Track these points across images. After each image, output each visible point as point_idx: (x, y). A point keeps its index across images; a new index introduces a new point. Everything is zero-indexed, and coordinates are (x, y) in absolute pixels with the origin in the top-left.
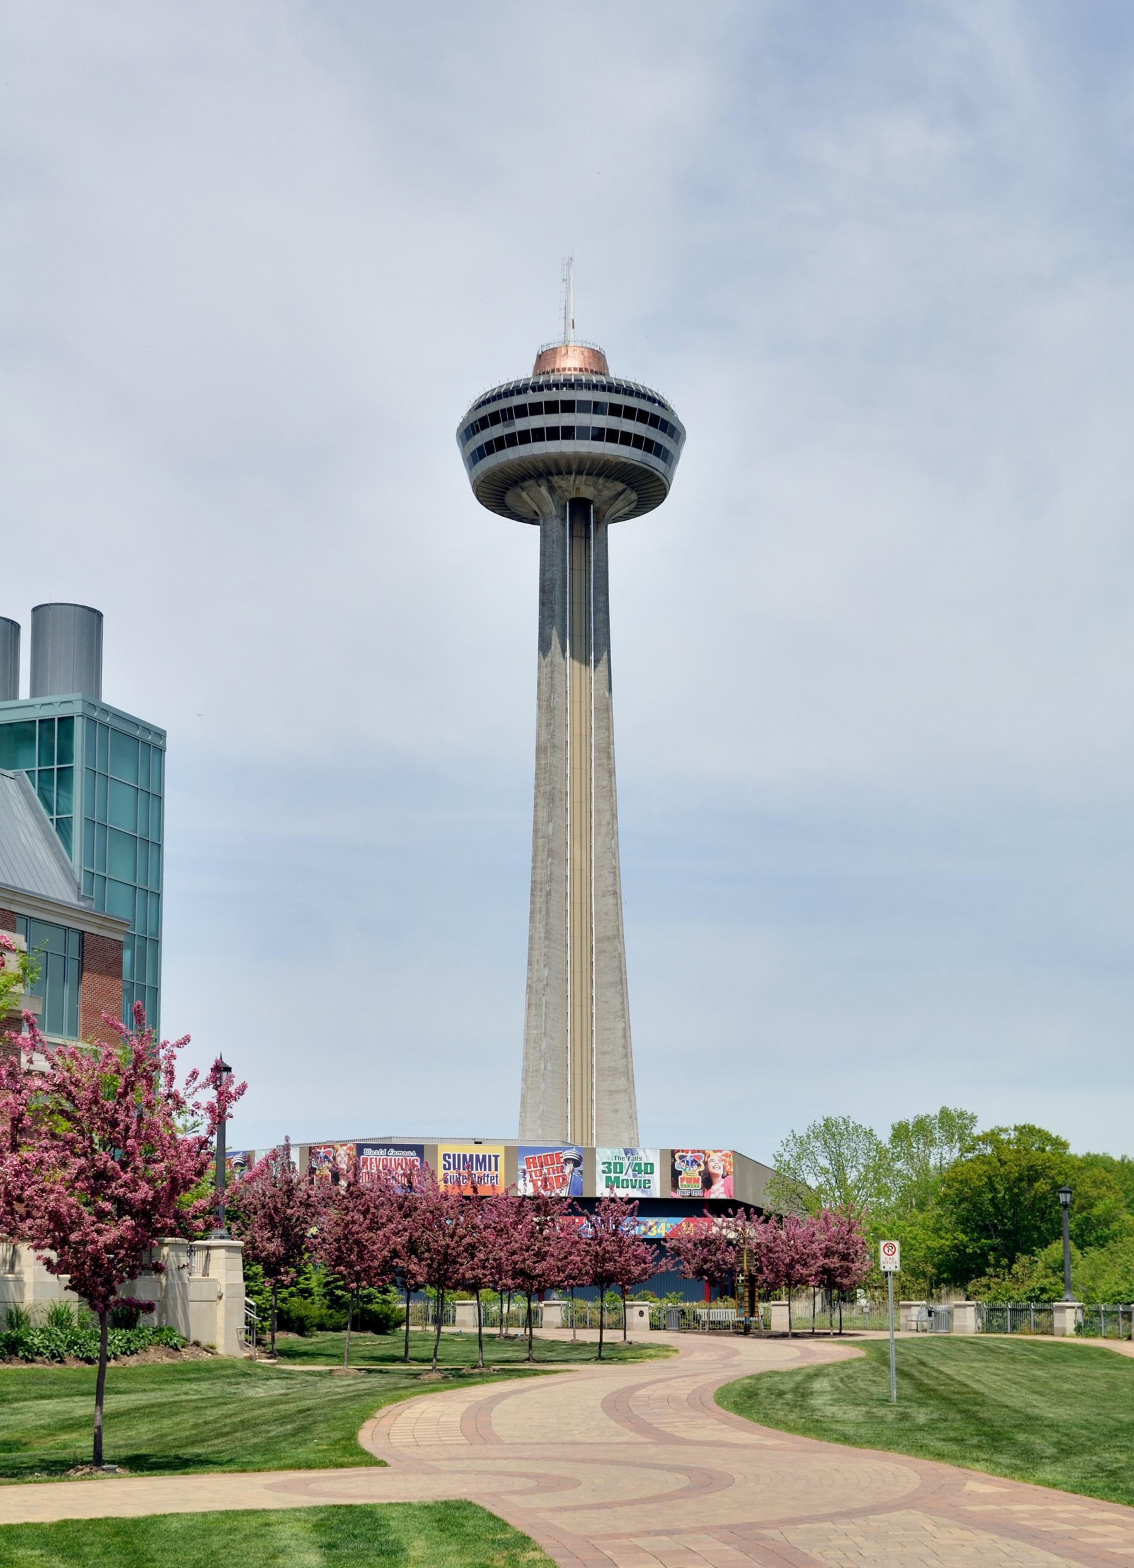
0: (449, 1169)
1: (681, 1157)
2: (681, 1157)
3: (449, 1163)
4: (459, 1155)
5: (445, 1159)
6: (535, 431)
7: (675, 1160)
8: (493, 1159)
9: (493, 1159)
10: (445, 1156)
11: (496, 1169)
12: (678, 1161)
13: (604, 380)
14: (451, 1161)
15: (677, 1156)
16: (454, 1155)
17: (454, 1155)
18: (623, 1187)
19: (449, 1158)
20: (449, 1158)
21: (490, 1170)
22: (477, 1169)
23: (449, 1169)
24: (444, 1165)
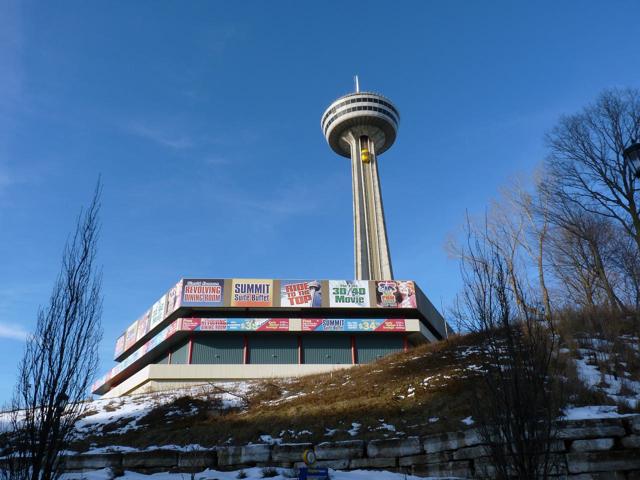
0: (239, 292)
1: (381, 285)
2: (381, 285)
3: (239, 289)
4: (245, 285)
7: (378, 287)
8: (266, 287)
9: (266, 287)
10: (236, 285)
12: (380, 287)
14: (240, 288)
15: (379, 284)
16: (242, 285)
17: (242, 285)
19: (239, 286)
21: (264, 292)
22: (256, 292)
23: (239, 292)
24: (236, 290)
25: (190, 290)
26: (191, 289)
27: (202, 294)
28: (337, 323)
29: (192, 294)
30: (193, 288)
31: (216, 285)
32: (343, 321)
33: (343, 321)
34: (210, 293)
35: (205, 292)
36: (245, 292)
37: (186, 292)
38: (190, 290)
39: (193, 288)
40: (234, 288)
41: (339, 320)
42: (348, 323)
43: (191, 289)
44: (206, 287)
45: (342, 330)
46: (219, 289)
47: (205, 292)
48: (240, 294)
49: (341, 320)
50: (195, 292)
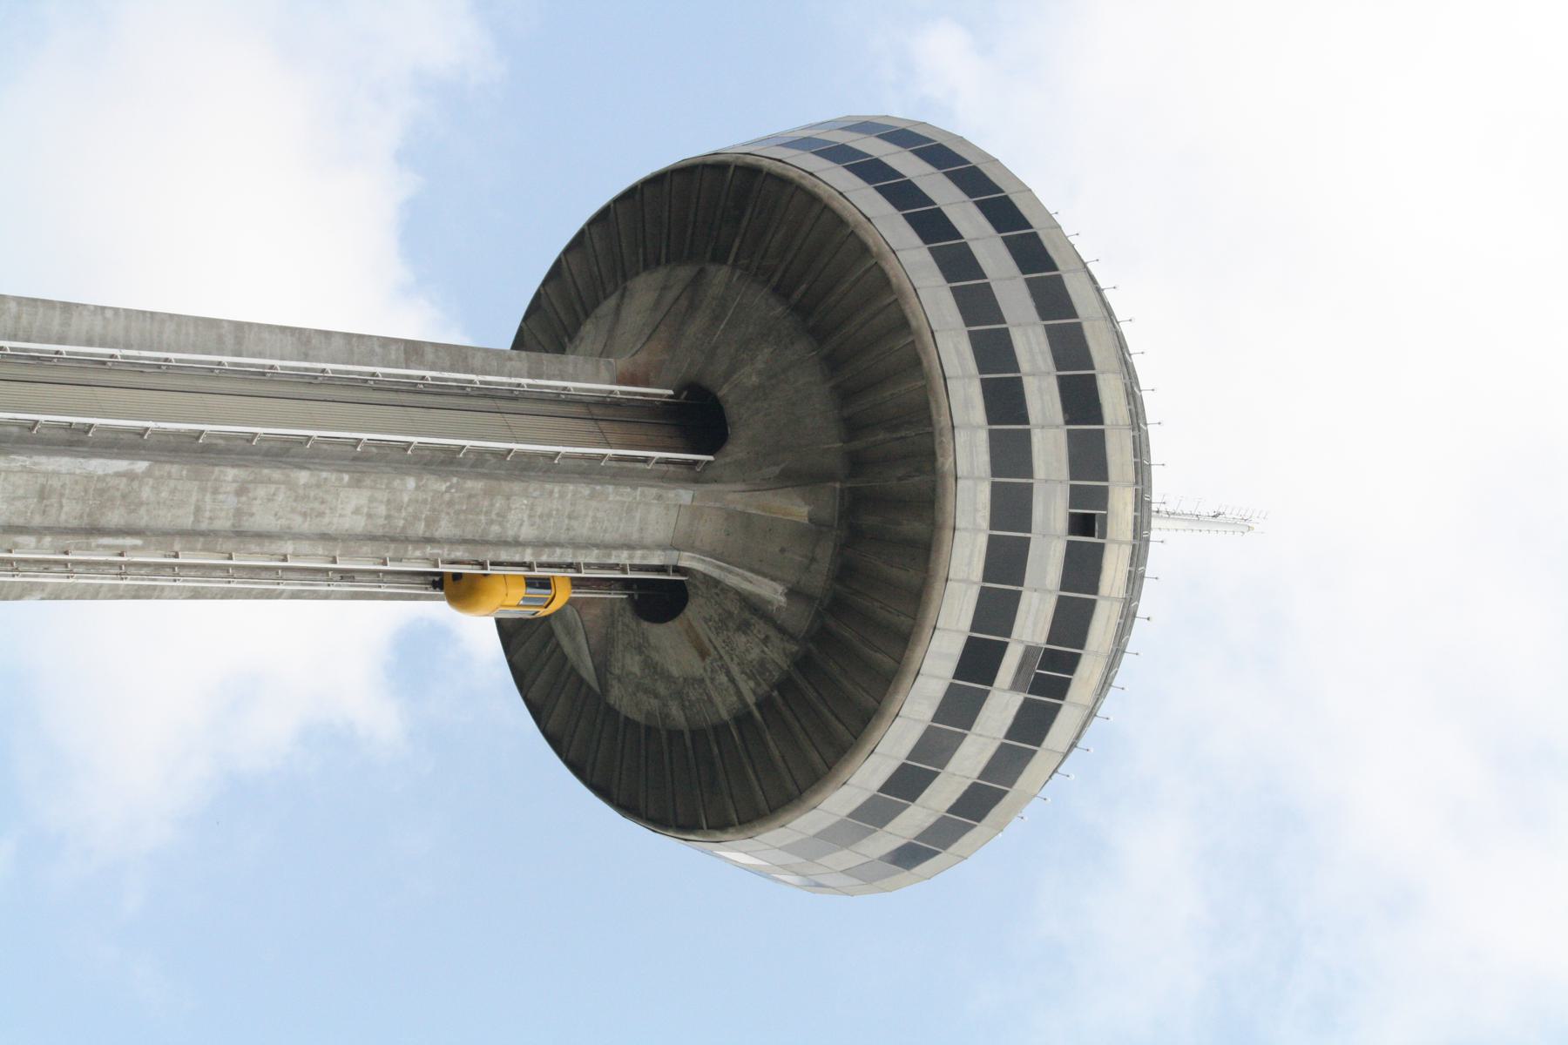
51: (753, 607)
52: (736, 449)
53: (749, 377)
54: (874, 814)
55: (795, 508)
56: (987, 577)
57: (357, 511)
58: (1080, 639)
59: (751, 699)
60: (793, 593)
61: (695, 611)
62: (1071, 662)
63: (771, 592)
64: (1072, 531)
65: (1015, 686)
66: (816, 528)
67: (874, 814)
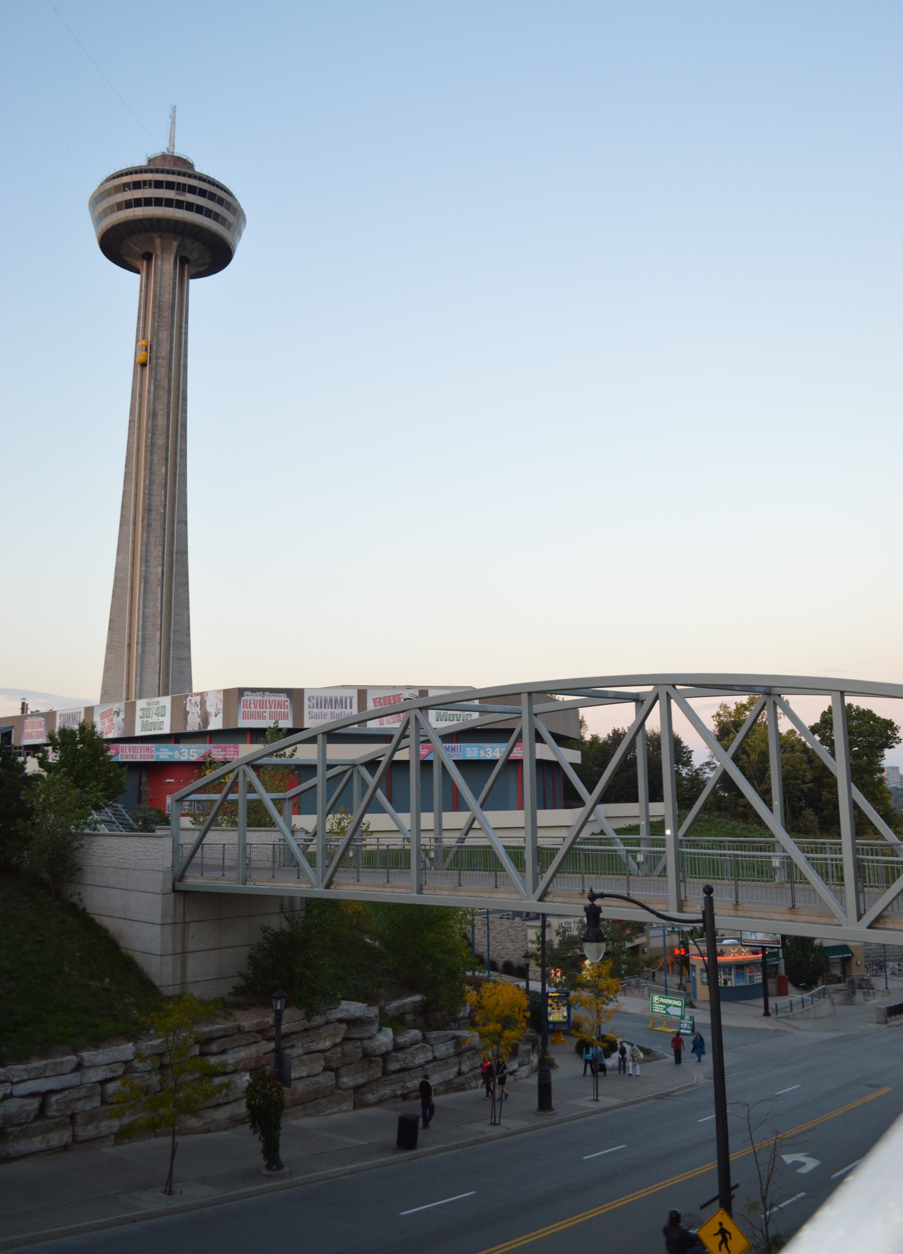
0: (313, 708)
5: (309, 700)
6: (146, 199)
11: (351, 708)
13: (190, 172)
18: (450, 720)
20: (314, 699)
21: (346, 708)
25: (248, 704)
26: (250, 704)
27: (264, 710)
28: (453, 749)
29: (252, 710)
30: (252, 701)
31: (283, 698)
32: (460, 746)
33: (460, 746)
34: (275, 708)
35: (268, 707)
36: (321, 708)
37: (244, 708)
38: (248, 704)
39: (252, 701)
40: (306, 703)
41: (456, 745)
42: (467, 749)
43: (250, 704)
44: (269, 700)
45: (459, 759)
46: (286, 704)
47: (268, 707)
48: (315, 710)
49: (459, 744)
50: (256, 708)
51: (180, 246)
52: (151, 251)
53: (137, 249)
54: (216, 217)
55: (158, 241)
56: (162, 206)
57: (162, 334)
58: (173, 183)
59: (199, 243)
60: (175, 240)
61: (185, 255)
62: (179, 184)
63: (175, 244)
64: (151, 188)
65: (184, 196)
66: (162, 238)
67: (216, 217)
